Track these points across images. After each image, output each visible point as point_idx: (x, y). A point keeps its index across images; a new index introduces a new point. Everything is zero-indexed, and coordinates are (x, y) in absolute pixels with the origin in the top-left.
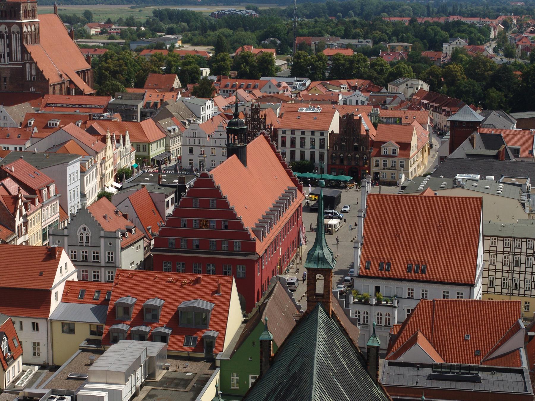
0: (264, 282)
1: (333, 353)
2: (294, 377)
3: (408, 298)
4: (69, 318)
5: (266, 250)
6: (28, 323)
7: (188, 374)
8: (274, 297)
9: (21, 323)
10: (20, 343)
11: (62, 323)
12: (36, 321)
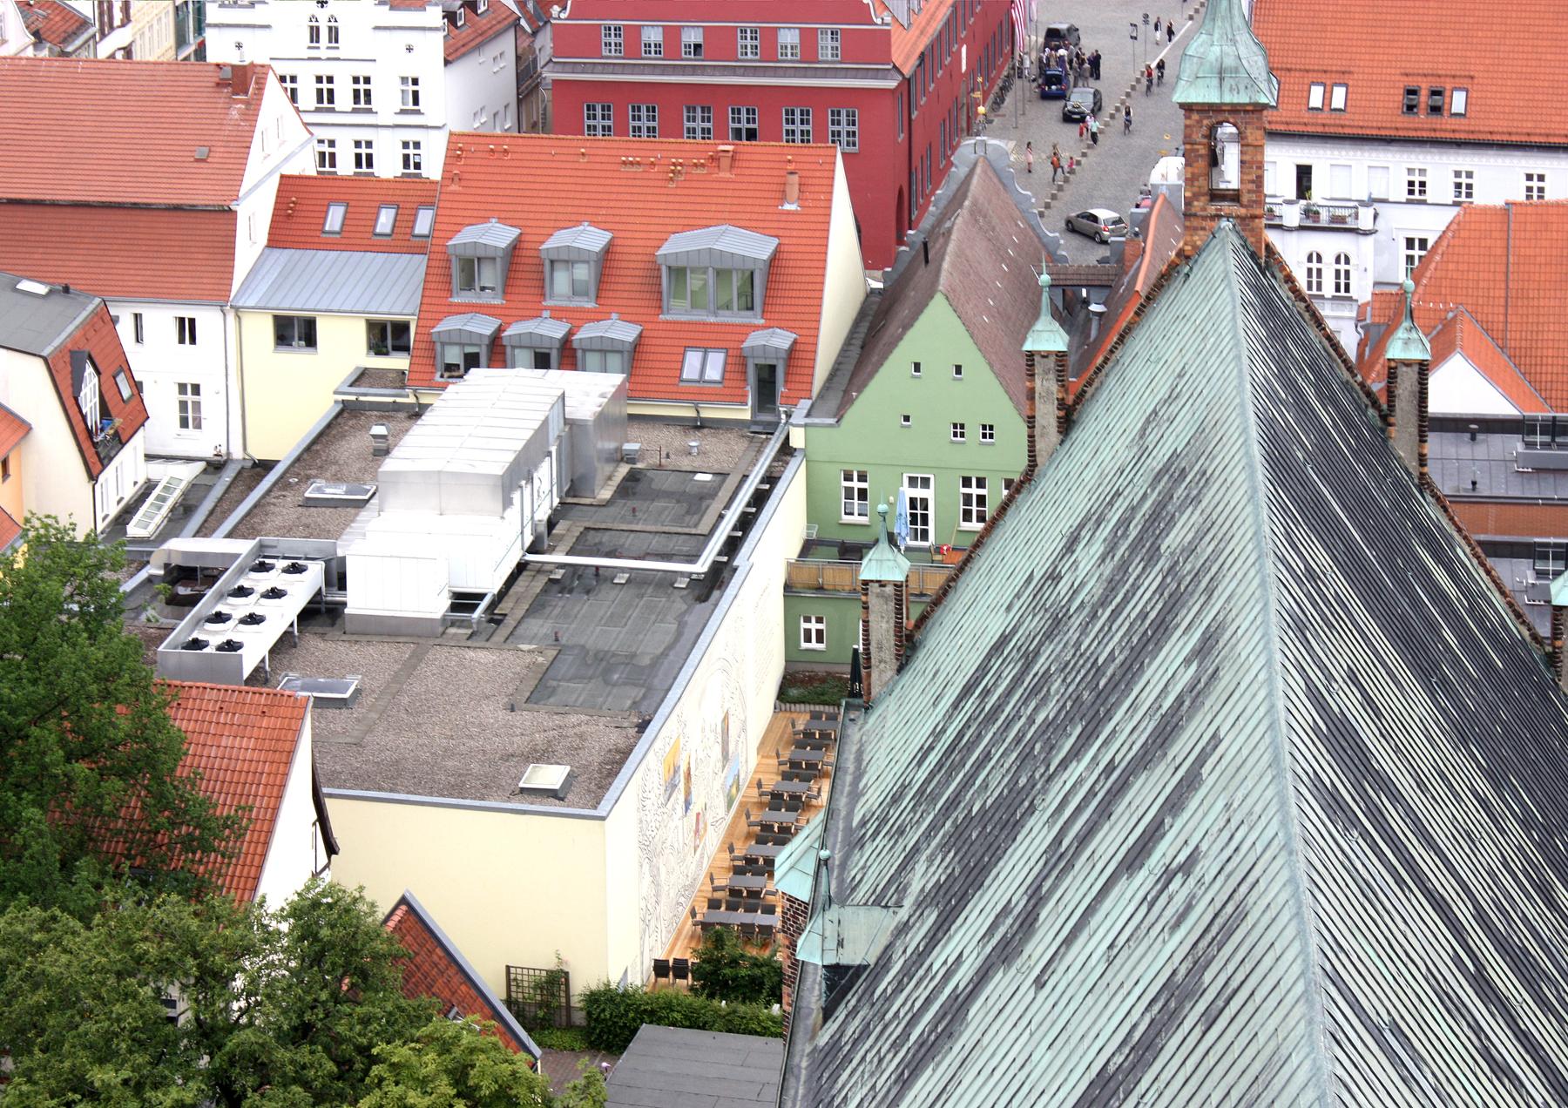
0: (916, 161)
1: (1290, 385)
2: (1173, 472)
3: (1409, 202)
4: (296, 304)
5: (922, 56)
6: (161, 320)
7: (699, 477)
8: (972, 213)
9: (137, 317)
10: (138, 387)
11: (276, 318)
12: (187, 313)
